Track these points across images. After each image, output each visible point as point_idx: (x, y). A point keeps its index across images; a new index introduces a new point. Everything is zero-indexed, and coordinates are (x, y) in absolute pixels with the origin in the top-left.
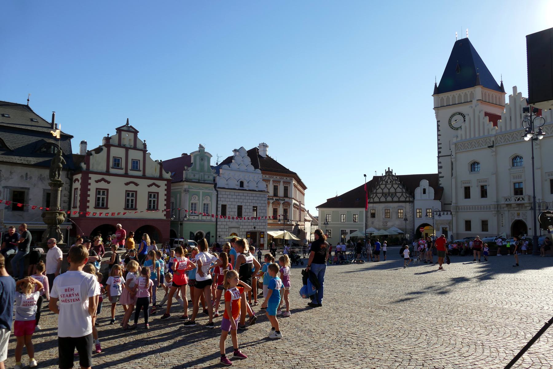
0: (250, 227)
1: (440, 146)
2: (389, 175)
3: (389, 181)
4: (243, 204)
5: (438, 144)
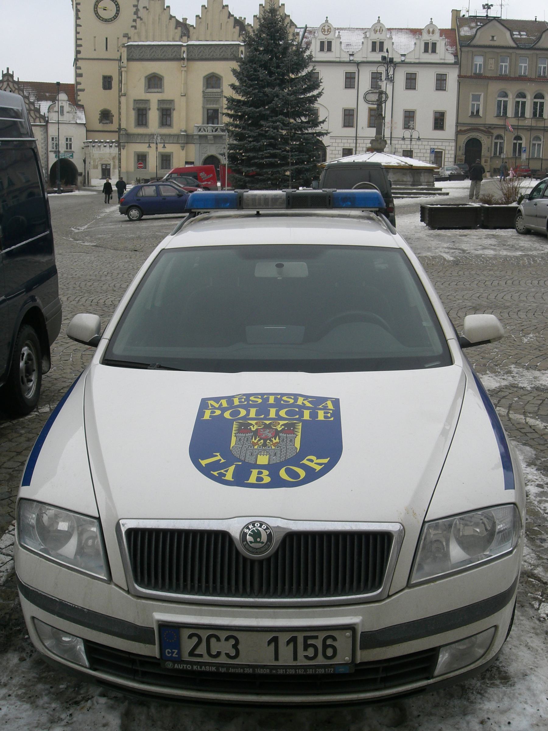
1: (79, 42)
2: (8, 80)
5: (77, 39)
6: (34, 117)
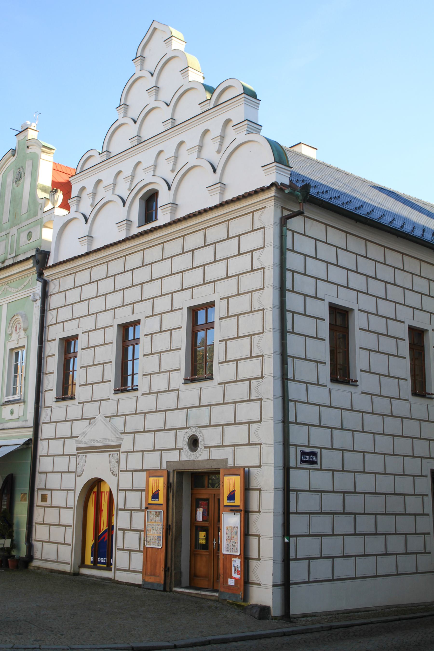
0: (166, 440)
4: (141, 311)
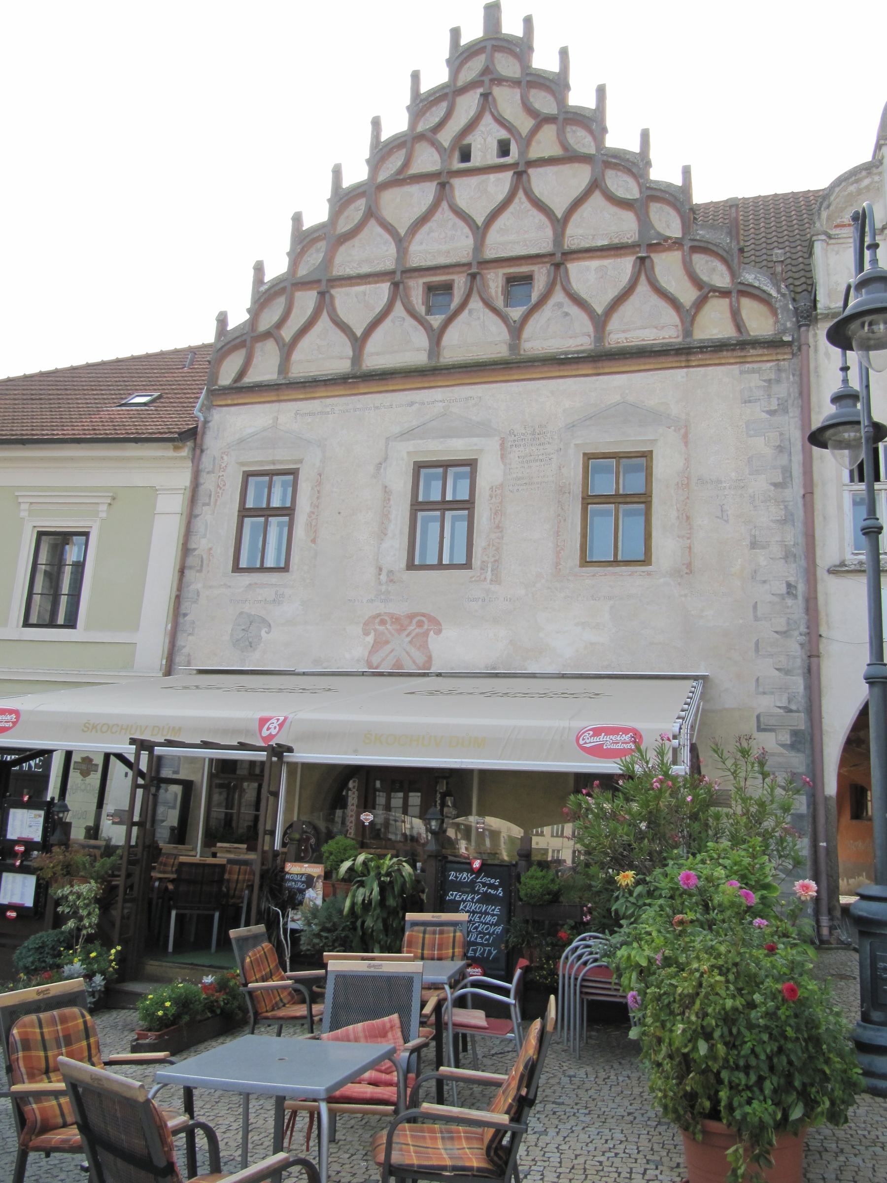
3: (484, 145)
6: (688, 295)
